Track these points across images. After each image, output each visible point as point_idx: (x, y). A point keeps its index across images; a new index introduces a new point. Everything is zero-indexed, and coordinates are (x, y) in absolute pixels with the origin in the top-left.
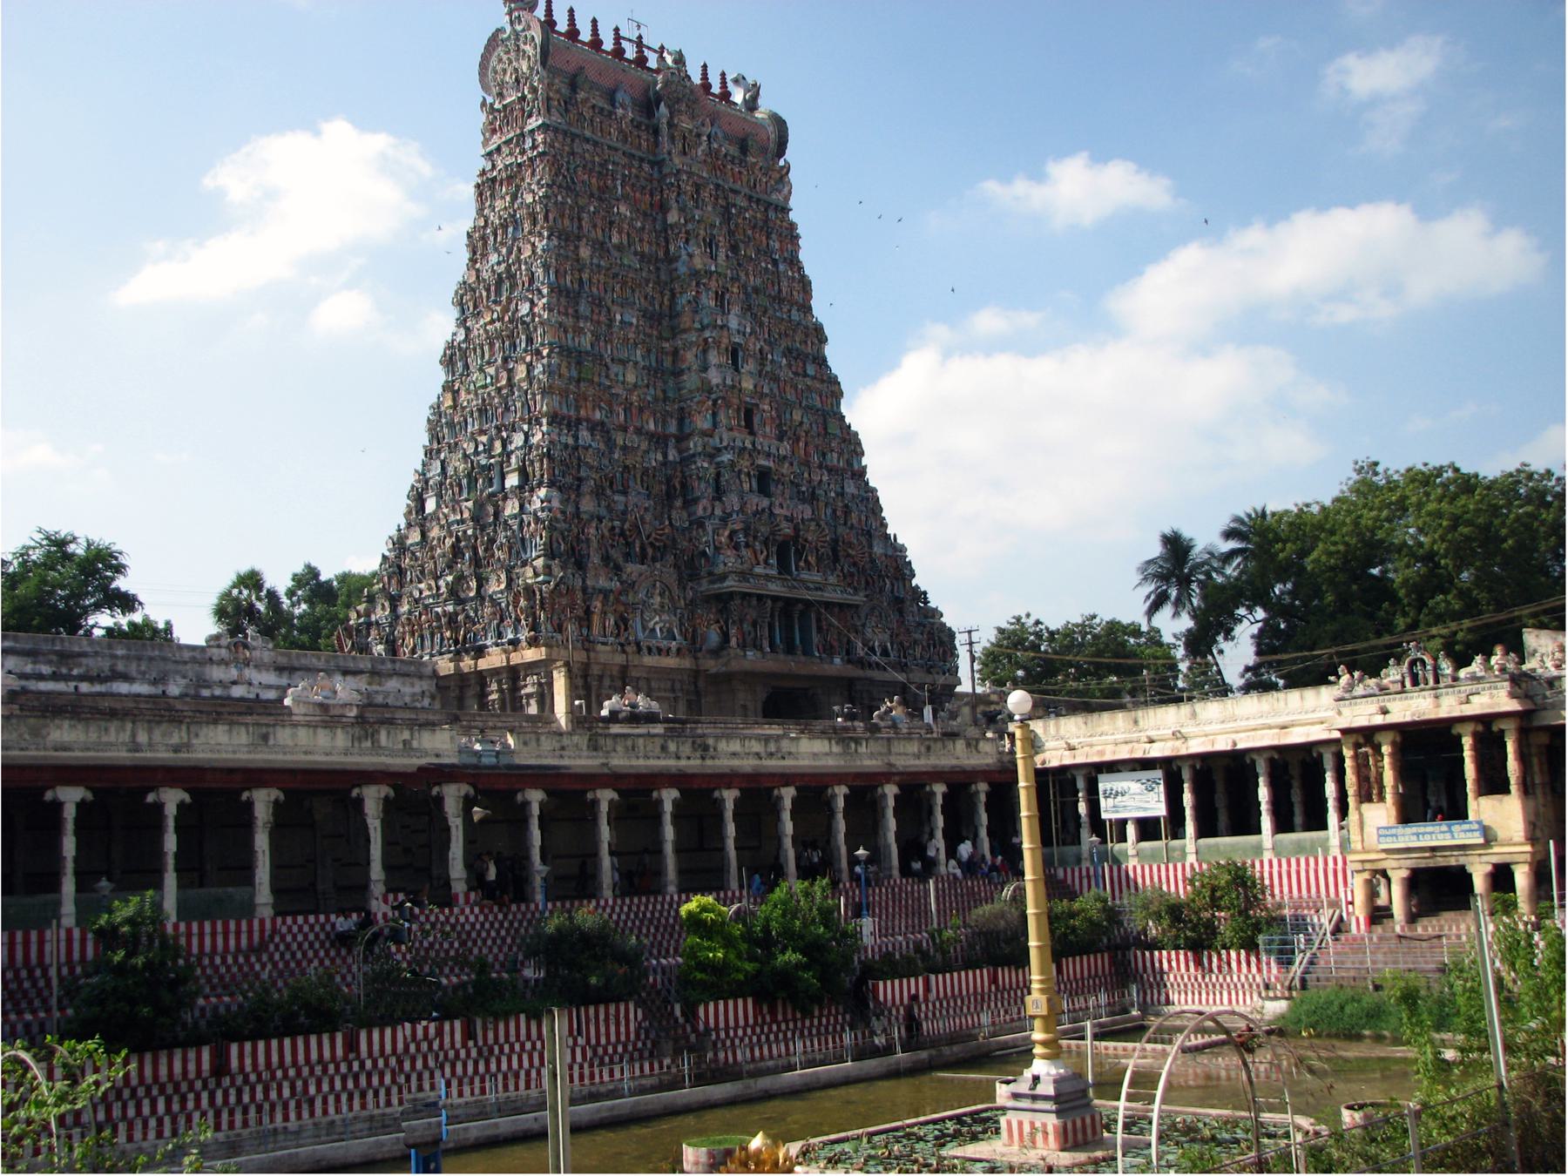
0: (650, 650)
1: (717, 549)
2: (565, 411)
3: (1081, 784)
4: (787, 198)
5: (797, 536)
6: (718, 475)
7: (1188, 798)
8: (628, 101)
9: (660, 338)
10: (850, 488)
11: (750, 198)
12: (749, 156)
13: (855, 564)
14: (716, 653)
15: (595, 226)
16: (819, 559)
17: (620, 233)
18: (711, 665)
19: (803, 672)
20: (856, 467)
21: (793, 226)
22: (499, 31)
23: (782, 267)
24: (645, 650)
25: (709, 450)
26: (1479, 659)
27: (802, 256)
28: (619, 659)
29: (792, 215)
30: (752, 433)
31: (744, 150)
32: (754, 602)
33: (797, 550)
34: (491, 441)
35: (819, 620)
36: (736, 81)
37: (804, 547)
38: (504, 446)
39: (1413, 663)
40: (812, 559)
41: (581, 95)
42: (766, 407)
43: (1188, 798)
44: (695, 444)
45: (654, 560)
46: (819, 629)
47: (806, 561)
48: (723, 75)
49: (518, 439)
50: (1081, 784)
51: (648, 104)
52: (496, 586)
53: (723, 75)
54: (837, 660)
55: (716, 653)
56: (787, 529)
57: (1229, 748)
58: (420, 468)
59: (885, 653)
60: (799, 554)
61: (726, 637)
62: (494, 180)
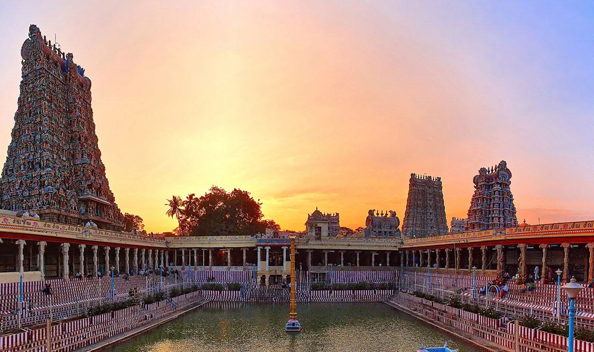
3: (183, 252)
6: (83, 170)
7: (210, 257)
34: (29, 155)
50: (183, 252)
60: (100, 192)
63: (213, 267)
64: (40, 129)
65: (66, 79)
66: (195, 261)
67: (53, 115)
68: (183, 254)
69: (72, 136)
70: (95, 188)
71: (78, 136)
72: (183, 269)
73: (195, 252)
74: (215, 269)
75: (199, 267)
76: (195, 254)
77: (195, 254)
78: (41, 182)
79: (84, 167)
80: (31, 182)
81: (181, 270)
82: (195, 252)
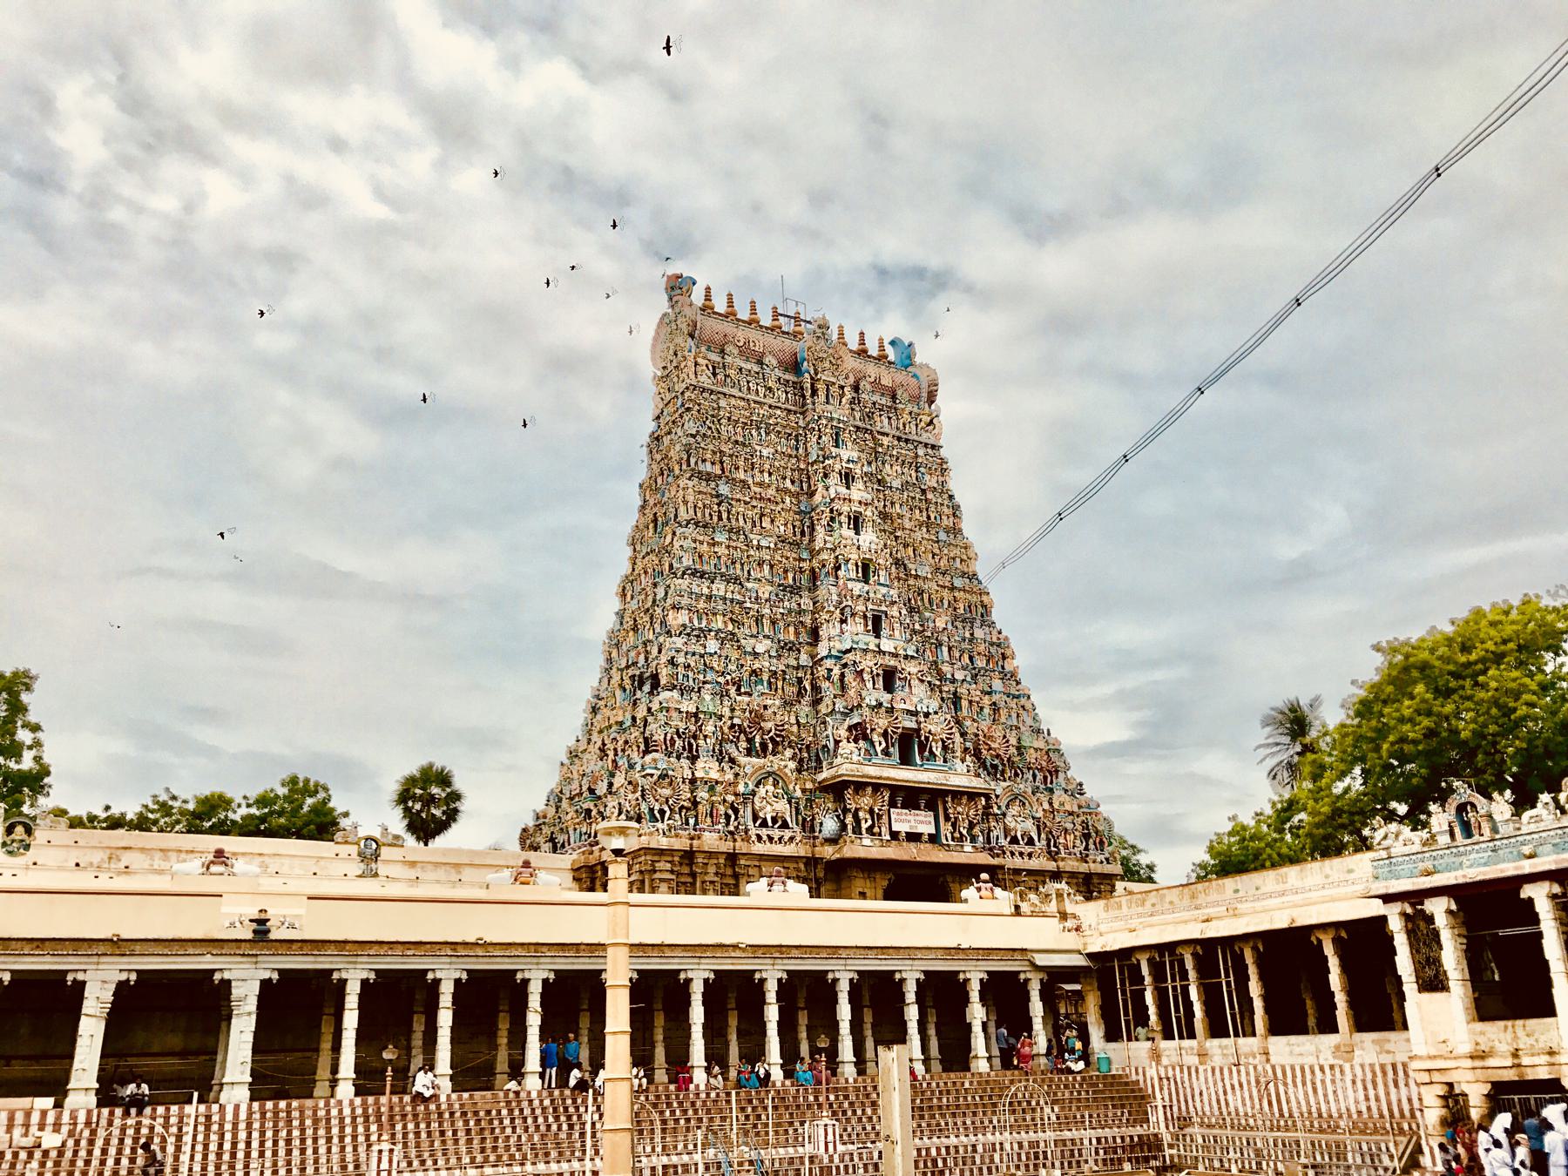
0: (759, 838)
1: (837, 742)
2: (696, 622)
4: (937, 437)
5: (918, 731)
6: (843, 675)
7: (1255, 989)
8: (774, 362)
9: (801, 560)
10: (997, 685)
11: (899, 439)
12: (894, 406)
13: (998, 756)
14: (832, 841)
15: (737, 468)
16: (945, 748)
17: (762, 472)
18: (828, 852)
19: (928, 859)
20: (1008, 668)
21: (943, 461)
22: (665, 315)
23: (930, 496)
24: (754, 838)
25: (834, 653)
26: (1545, 797)
27: (954, 485)
28: (726, 847)
29: (943, 453)
30: (878, 636)
31: (894, 397)
32: (869, 790)
33: (920, 743)
35: (946, 809)
36: (893, 343)
37: (927, 738)
38: (646, 659)
39: (1461, 809)
40: (938, 752)
41: (729, 359)
42: (896, 614)
43: (1255, 989)
44: (822, 650)
45: (774, 753)
46: (947, 818)
47: (931, 752)
48: (881, 340)
49: (655, 651)
51: (794, 366)
52: (619, 780)
53: (881, 340)
54: (968, 848)
55: (832, 841)
56: (910, 724)
57: (1285, 925)
58: (596, 684)
59: (1031, 842)
61: (843, 827)
62: (657, 439)
63: (1273, 1040)
64: (671, 566)
65: (804, 396)
66: (1198, 1009)
67: (725, 516)
68: (1148, 980)
69: (812, 570)
70: (885, 734)
71: (830, 567)
72: (1156, 1056)
73: (1189, 964)
74: (1290, 1050)
75: (1216, 1042)
76: (1192, 975)
77: (1192, 975)
78: (646, 740)
79: (845, 666)
80: (626, 742)
81: (1146, 1062)
82: (1189, 964)
